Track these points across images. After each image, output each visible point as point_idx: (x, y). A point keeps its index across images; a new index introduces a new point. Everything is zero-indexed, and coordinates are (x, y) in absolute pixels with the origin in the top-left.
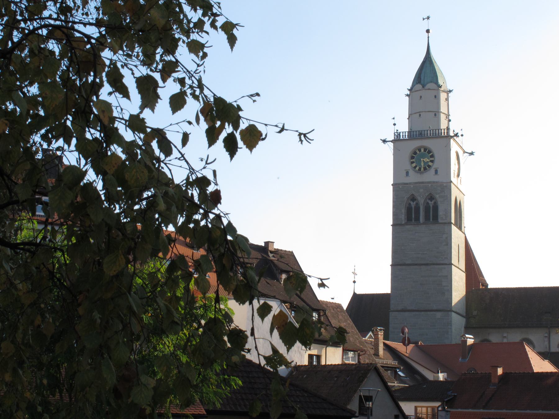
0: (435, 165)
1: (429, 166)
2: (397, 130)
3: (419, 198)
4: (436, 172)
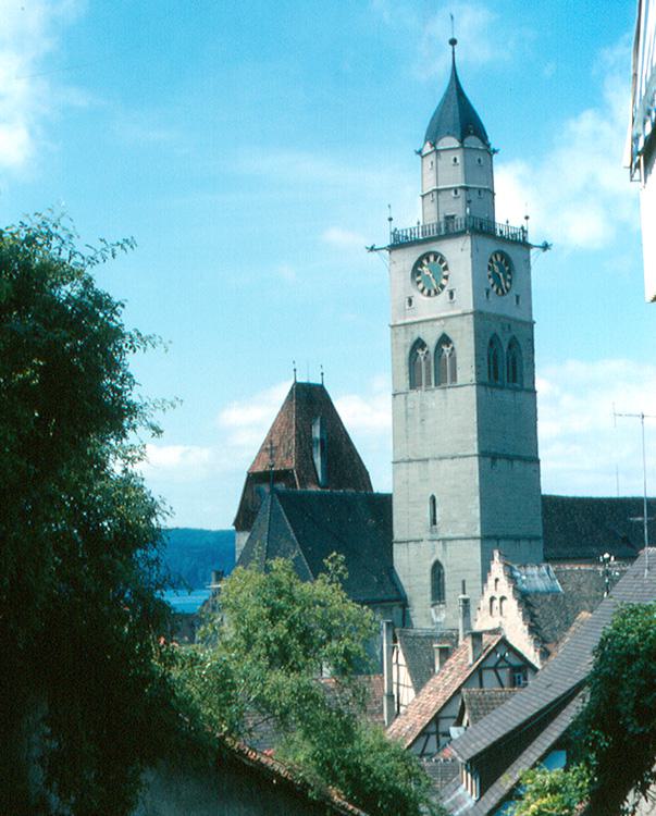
1: (442, 287)
4: (451, 294)
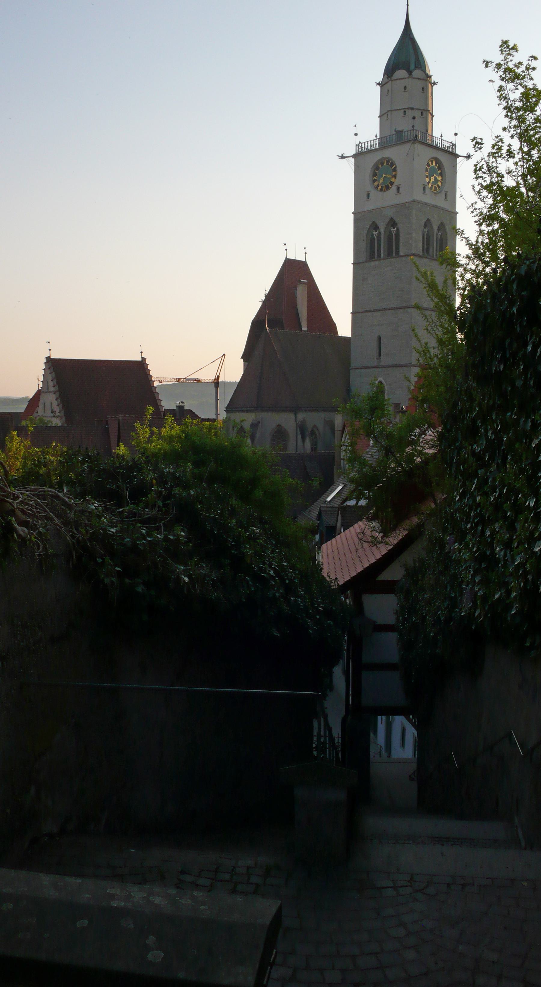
0: (397, 182)
1: (392, 183)
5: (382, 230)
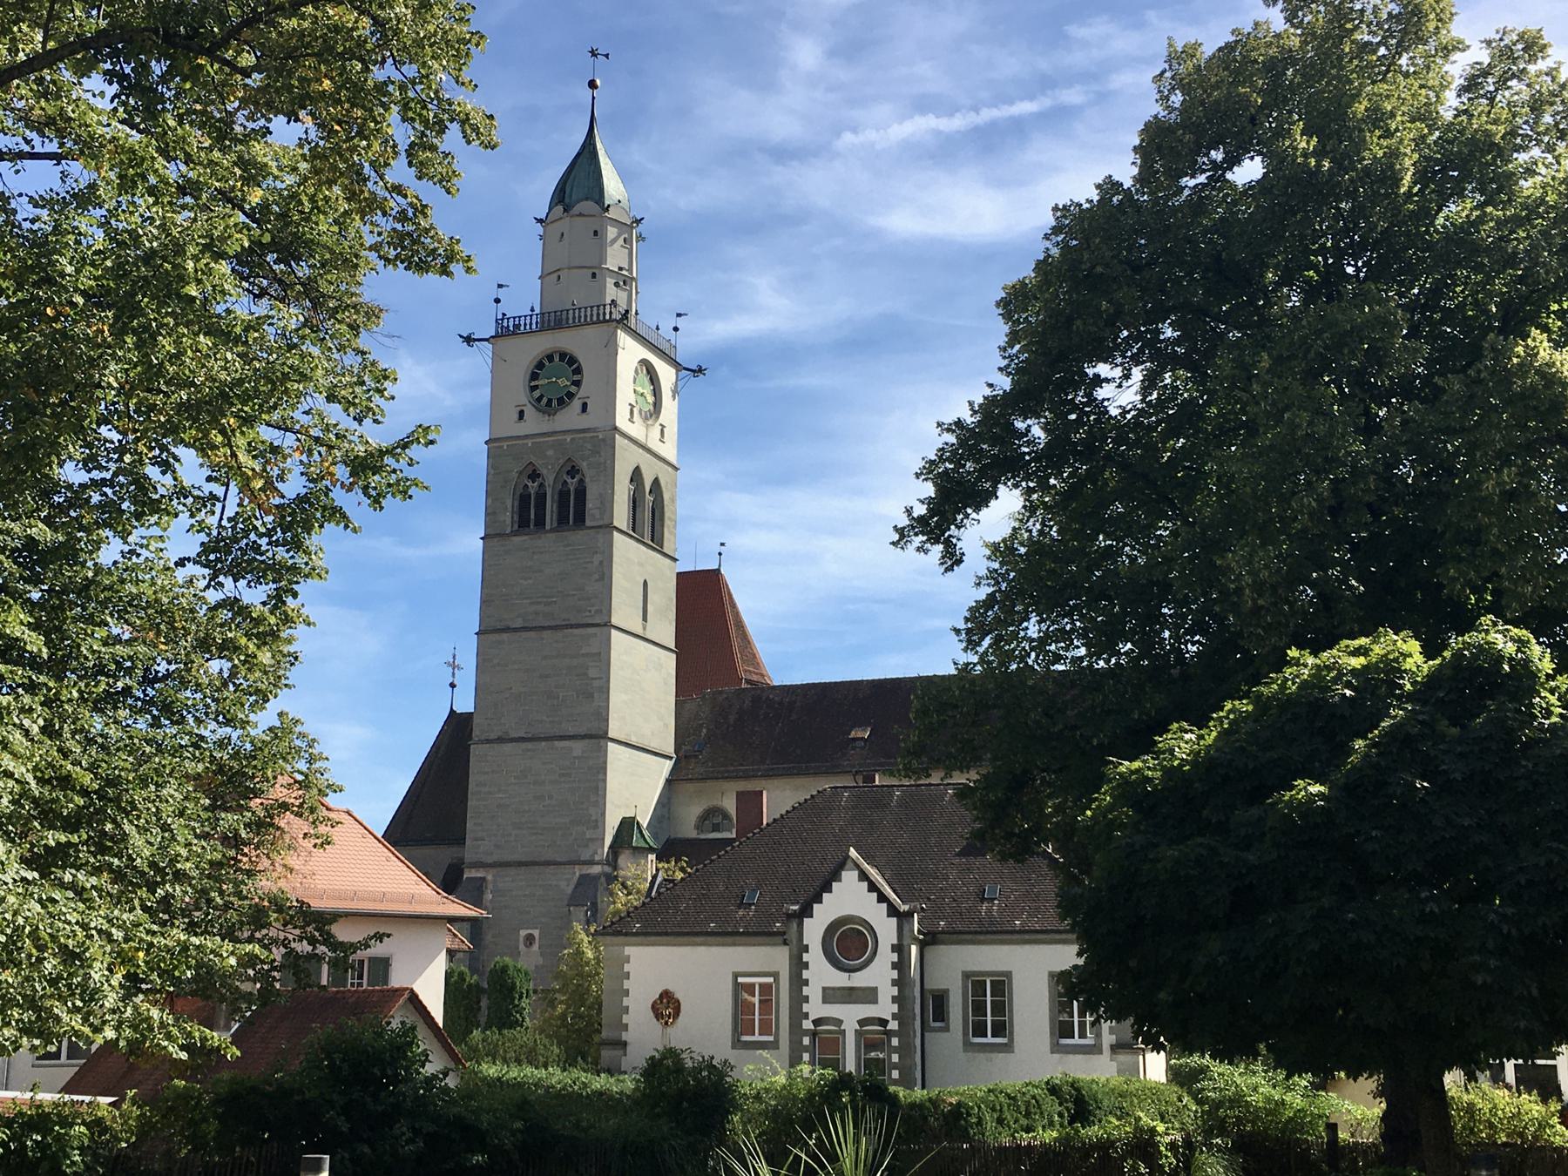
2: (504, 315)
3: (544, 472)
4: (584, 407)
5: (549, 480)
